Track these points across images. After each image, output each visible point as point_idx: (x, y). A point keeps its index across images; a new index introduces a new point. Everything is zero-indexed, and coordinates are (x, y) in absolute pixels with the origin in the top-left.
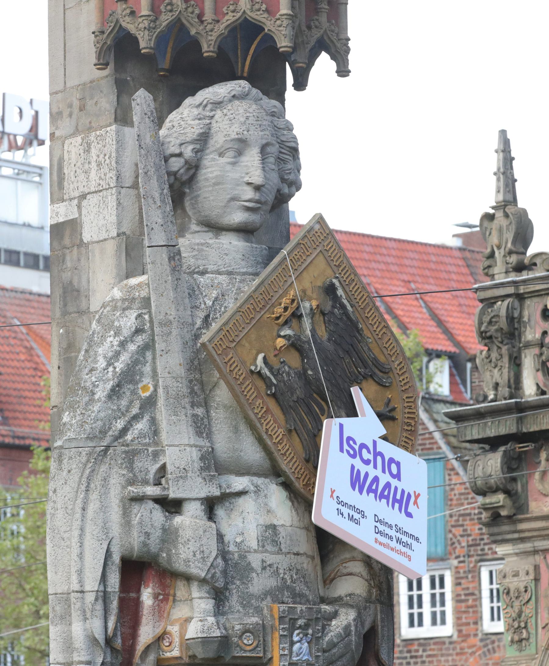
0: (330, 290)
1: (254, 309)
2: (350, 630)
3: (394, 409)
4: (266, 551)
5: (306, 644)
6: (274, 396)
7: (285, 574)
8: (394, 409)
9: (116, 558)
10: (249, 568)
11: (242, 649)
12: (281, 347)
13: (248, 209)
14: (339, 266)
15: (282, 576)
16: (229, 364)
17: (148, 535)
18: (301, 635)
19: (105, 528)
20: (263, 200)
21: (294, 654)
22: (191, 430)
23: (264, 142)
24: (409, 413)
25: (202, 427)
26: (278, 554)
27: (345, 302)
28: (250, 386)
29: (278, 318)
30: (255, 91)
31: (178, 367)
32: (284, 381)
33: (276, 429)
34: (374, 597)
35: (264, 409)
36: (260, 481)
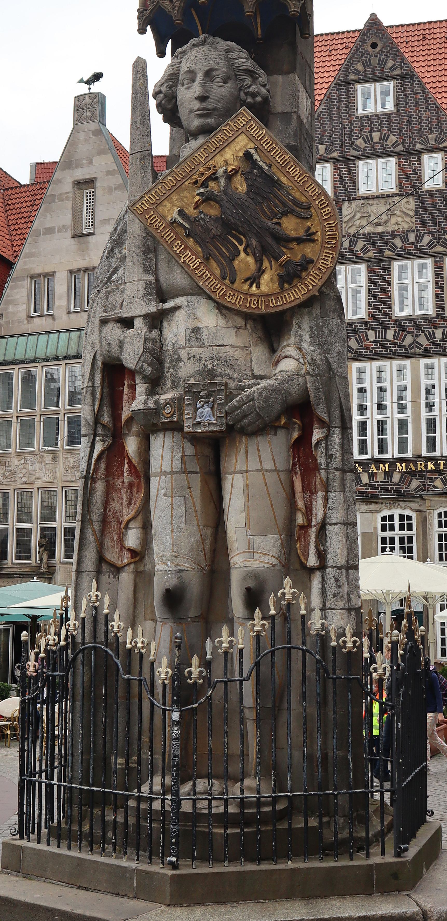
0: (248, 156)
1: (176, 179)
2: (254, 397)
3: (314, 233)
4: (192, 346)
5: (208, 409)
6: (188, 236)
7: (206, 361)
8: (314, 233)
9: (99, 363)
10: (179, 360)
11: (165, 417)
12: (197, 202)
13: (200, 116)
14: (261, 140)
15: (203, 362)
16: (149, 220)
17: (109, 344)
18: (202, 403)
19: (93, 345)
20: (209, 107)
21: (198, 417)
22: (141, 270)
23: (207, 68)
24: (329, 235)
25: (150, 267)
26: (201, 347)
27: (261, 163)
28: (170, 232)
29: (196, 182)
30: (211, 39)
31: (137, 229)
32: (201, 226)
33: (194, 259)
34: (303, 371)
35: (183, 247)
36: (192, 298)
